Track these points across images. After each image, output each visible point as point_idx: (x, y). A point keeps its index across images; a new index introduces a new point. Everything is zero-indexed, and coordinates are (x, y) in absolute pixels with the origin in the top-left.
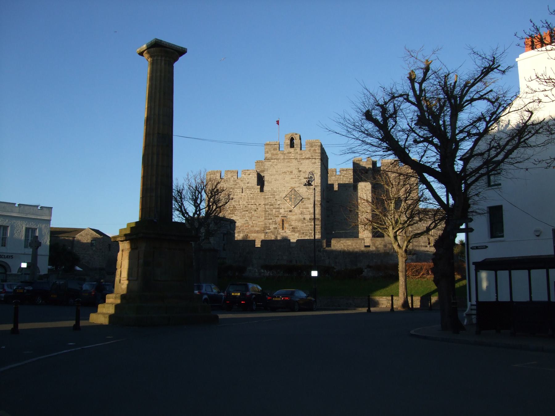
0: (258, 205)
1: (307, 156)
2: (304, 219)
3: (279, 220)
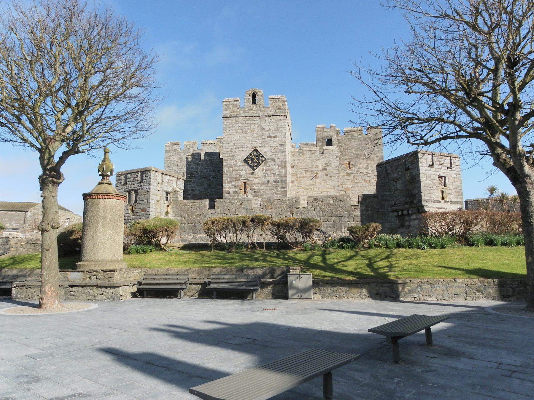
0: (217, 171)
1: (271, 113)
2: (268, 181)
3: (240, 183)
